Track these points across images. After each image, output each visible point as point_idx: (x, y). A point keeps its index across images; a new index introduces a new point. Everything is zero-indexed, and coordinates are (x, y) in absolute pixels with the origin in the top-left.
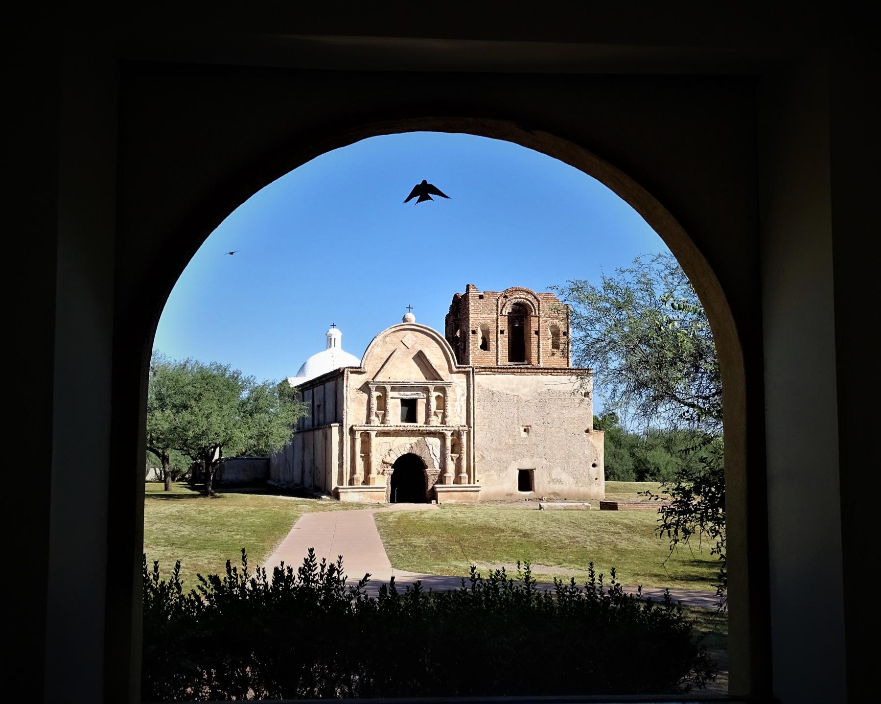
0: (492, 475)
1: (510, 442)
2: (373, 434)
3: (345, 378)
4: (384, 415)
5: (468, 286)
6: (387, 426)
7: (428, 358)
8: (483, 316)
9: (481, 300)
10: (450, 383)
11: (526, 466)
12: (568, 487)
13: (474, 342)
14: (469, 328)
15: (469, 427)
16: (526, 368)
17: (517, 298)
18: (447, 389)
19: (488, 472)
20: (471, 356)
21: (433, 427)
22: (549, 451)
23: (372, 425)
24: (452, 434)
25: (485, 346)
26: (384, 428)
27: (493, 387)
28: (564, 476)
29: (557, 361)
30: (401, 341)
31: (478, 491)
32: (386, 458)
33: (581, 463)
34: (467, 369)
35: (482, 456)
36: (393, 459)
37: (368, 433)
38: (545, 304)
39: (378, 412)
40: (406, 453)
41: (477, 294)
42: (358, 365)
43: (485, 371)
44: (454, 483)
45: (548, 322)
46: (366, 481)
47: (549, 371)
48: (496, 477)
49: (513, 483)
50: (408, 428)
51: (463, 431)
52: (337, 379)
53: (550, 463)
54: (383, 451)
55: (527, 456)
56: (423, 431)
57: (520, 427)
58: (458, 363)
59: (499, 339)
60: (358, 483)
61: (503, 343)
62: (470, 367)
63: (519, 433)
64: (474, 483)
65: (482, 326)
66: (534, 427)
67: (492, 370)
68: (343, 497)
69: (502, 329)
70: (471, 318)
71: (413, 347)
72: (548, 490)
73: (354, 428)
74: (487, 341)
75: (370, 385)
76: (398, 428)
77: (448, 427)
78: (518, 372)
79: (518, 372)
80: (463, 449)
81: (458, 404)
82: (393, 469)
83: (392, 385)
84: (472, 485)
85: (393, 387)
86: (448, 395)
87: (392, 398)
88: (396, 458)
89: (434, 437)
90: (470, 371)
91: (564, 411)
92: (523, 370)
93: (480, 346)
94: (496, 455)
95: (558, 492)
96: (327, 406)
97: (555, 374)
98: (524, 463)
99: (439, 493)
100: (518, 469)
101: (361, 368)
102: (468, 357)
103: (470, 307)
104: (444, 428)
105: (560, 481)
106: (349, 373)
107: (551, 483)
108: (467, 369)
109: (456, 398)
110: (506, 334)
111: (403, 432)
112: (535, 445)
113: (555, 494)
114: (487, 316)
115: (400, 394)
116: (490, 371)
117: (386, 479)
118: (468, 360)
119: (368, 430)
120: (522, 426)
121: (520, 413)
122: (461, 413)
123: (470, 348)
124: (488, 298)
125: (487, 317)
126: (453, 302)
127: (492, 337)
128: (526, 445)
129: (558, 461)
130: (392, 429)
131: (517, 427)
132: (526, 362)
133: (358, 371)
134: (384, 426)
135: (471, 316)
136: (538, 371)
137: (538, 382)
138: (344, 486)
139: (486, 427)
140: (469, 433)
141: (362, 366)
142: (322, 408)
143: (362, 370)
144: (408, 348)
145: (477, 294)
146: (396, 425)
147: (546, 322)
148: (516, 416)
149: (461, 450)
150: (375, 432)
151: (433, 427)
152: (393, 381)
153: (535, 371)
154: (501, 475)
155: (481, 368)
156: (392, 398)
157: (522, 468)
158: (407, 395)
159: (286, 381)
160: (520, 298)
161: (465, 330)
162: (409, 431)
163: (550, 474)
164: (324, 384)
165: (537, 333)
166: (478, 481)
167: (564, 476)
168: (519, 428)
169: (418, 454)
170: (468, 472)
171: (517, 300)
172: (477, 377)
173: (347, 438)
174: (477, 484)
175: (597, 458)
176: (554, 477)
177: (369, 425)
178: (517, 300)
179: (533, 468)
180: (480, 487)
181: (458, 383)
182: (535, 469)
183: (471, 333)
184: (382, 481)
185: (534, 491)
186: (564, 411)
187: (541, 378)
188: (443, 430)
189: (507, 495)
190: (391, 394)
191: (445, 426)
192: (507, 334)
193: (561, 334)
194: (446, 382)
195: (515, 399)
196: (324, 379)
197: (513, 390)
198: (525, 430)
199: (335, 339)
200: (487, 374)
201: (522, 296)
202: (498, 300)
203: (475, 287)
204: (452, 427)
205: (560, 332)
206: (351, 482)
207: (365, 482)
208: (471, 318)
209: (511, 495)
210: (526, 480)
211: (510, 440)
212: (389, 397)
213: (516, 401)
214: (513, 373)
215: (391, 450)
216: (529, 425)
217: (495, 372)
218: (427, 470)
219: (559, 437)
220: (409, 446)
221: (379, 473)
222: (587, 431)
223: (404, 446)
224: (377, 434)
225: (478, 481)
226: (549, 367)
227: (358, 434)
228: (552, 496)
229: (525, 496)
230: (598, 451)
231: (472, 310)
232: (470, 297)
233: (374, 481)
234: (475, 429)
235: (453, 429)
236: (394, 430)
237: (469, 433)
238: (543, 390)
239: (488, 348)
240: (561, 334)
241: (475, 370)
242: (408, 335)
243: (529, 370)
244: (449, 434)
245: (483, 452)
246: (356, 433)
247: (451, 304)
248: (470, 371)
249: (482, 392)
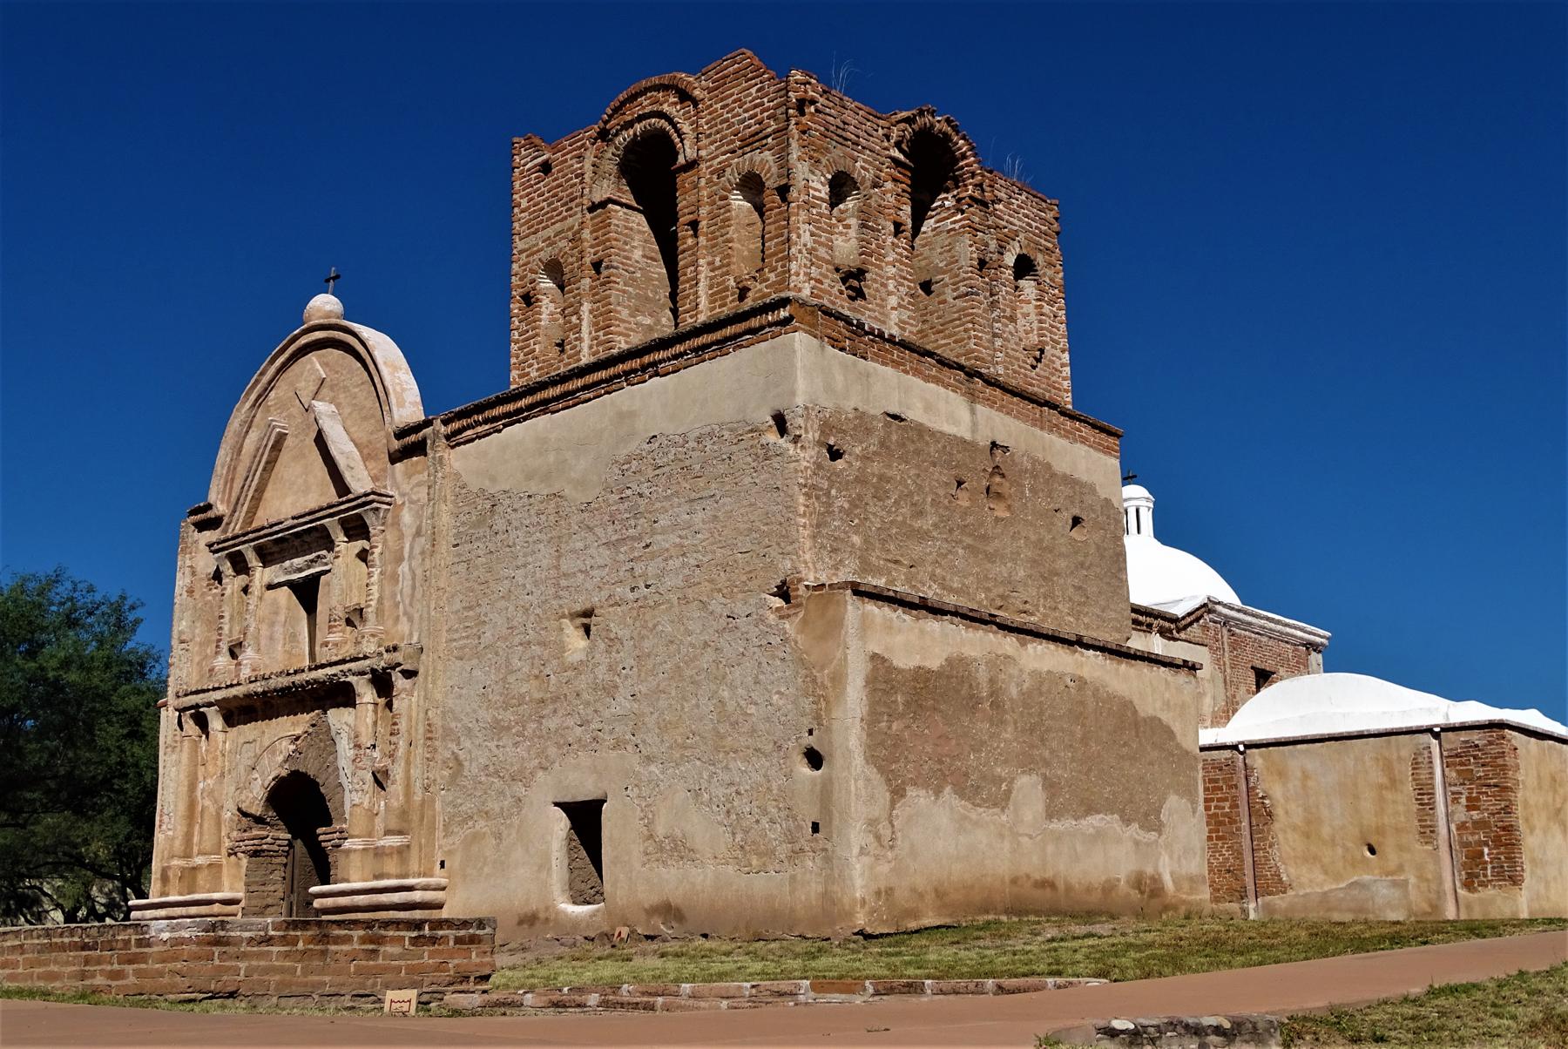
19: (470, 823)
27: (493, 479)
38: (719, 106)
40: (284, 773)
41: (536, 161)
43: (470, 427)
47: (646, 359)
78: (556, 399)
81: (406, 569)
83: (252, 544)
89: (345, 706)
92: (571, 386)
94: (494, 749)
95: (676, 899)
97: (669, 366)
100: (556, 804)
115: (287, 572)
116: (486, 421)
122: (411, 605)
136: (612, 371)
137: (625, 416)
138: (152, 900)
145: (536, 161)
147: (720, 172)
153: (603, 374)
158: (300, 570)
166: (442, 864)
171: (631, 132)
175: (818, 718)
176: (660, 830)
187: (627, 397)
197: (547, 478)
200: (479, 437)
214: (544, 406)
216: (588, 606)
217: (495, 419)
218: (319, 831)
222: (784, 592)
230: (824, 687)
231: (521, 226)
236: (248, 696)
238: (631, 448)
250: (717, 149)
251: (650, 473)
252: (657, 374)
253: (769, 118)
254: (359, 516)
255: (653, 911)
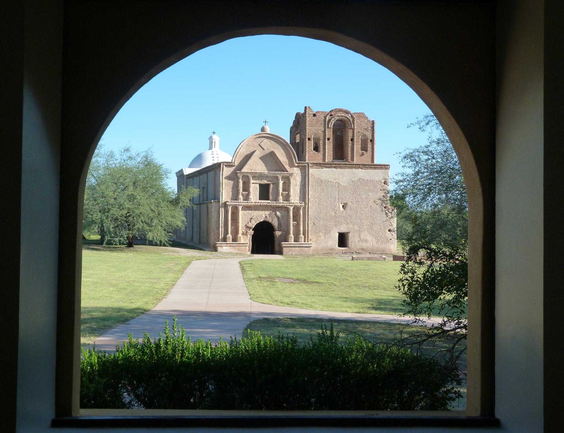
0: (320, 236)
1: (333, 214)
2: (240, 208)
3: (221, 170)
4: (248, 195)
5: (306, 108)
6: (250, 202)
7: (278, 156)
8: (316, 128)
9: (315, 117)
10: (292, 173)
11: (343, 230)
12: (371, 244)
13: (309, 146)
14: (306, 136)
15: (305, 204)
16: (344, 164)
17: (339, 116)
18: (290, 178)
19: (317, 234)
20: (307, 155)
21: (280, 203)
22: (359, 221)
23: (239, 201)
24: (294, 208)
25: (316, 149)
26: (247, 204)
27: (322, 176)
28: (369, 238)
29: (366, 159)
30: (259, 145)
31: (310, 247)
32: (248, 224)
33: (380, 228)
34: (304, 165)
35: (314, 223)
36: (253, 224)
37: (236, 207)
39: (244, 193)
40: (262, 221)
41: (312, 113)
42: (230, 161)
44: (294, 242)
45: (360, 133)
46: (235, 239)
48: (323, 238)
49: (334, 242)
50: (264, 204)
51: (301, 206)
52: (216, 170)
53: (360, 229)
54: (247, 219)
55: (344, 223)
56: (274, 205)
57: (340, 204)
58: (298, 160)
59: (327, 144)
60: (230, 240)
61: (329, 147)
62: (306, 163)
63: (339, 208)
64: (308, 242)
65: (315, 134)
66: (349, 204)
67: (322, 165)
68: (219, 249)
69: (328, 137)
70: (308, 129)
71: (267, 149)
72: (358, 247)
73: (227, 203)
74: (318, 145)
75: (238, 174)
76: (257, 204)
77: (291, 203)
79: (339, 167)
80: (301, 218)
82: (253, 231)
84: (307, 243)
85: (254, 176)
86: (291, 182)
87: (253, 183)
88: (256, 224)
90: (305, 166)
91: (370, 194)
93: (313, 150)
95: (365, 248)
96: (209, 188)
98: (342, 229)
99: (284, 248)
101: (232, 162)
102: (305, 156)
103: (307, 122)
104: (288, 204)
105: (366, 241)
106: (224, 166)
107: (360, 242)
108: (304, 165)
109: (297, 184)
110: (331, 140)
111: (260, 207)
112: (350, 216)
113: (363, 249)
114: (318, 128)
117: (249, 238)
118: (305, 158)
119: (236, 205)
120: (341, 203)
121: (339, 194)
123: (307, 150)
124: (319, 116)
125: (318, 129)
126: (295, 118)
127: (321, 142)
128: (344, 216)
129: (365, 227)
130: (253, 204)
131: (338, 204)
132: (345, 160)
133: (229, 165)
134: (247, 202)
135: (307, 128)
139: (317, 204)
140: (304, 208)
141: (233, 161)
142: (205, 189)
143: (233, 164)
144: (264, 149)
145: (312, 113)
146: (255, 201)
147: (358, 132)
148: (337, 197)
149: (300, 219)
150: (241, 207)
151: (280, 203)
152: (254, 172)
154: (326, 236)
155: (314, 164)
156: (252, 183)
157: (341, 231)
159: (182, 170)
160: (341, 116)
161: (303, 138)
162: (264, 205)
163: (359, 236)
164: (207, 173)
165: (352, 140)
166: (310, 240)
167: (369, 238)
168: (339, 205)
169: (270, 221)
170: (304, 234)
171: (339, 117)
172: (311, 170)
173: (222, 210)
174: (310, 242)
176: (362, 238)
177: (237, 201)
178: (339, 117)
179: (348, 232)
180: (312, 244)
181: (296, 173)
182: (349, 232)
183: (307, 139)
184: (246, 240)
185: (349, 248)
186: (370, 194)
187: (354, 170)
188: (287, 205)
189: (330, 250)
190: (252, 181)
191: (289, 202)
192: (332, 141)
193: (369, 141)
194: (290, 172)
195: (337, 185)
196: (207, 170)
197: (335, 179)
198: (343, 206)
199: (215, 142)
201: (342, 115)
202: (325, 117)
203: (310, 108)
204: (294, 203)
205: (368, 139)
206: (225, 239)
207: (235, 240)
208: (308, 129)
209: (333, 249)
210: (343, 240)
211: (333, 212)
212: (251, 183)
213: (337, 187)
215: (251, 219)
217: (323, 166)
219: (366, 211)
220: (264, 216)
221: (243, 234)
223: (261, 216)
224: (242, 207)
225: (310, 240)
226: (361, 163)
227: (230, 207)
228: (361, 251)
229: (342, 250)
232: (307, 115)
233: (240, 239)
234: (309, 205)
235: (294, 204)
236: (254, 205)
237: (304, 208)
239: (319, 150)
240: (369, 141)
241: (310, 165)
242: (264, 140)
243: (347, 166)
244: (292, 208)
245: (314, 220)
246: (229, 207)
247: (294, 119)
248: (306, 166)
249: (314, 180)
250: (358, 128)
251: (359, 184)
252: (362, 169)
253: (369, 127)
254: (288, 177)
255: (359, 249)
